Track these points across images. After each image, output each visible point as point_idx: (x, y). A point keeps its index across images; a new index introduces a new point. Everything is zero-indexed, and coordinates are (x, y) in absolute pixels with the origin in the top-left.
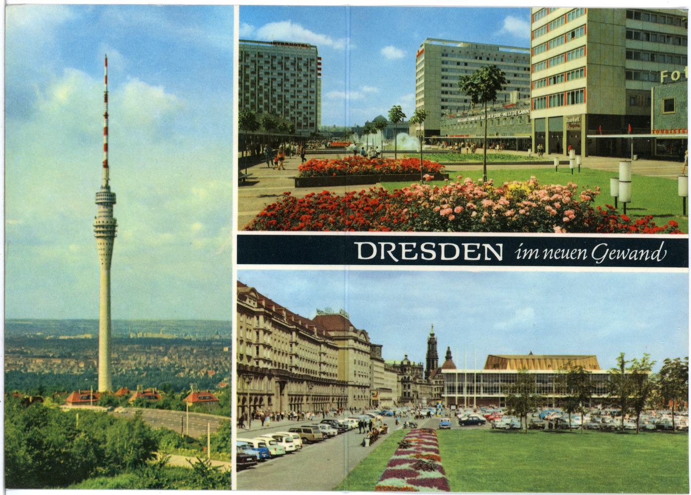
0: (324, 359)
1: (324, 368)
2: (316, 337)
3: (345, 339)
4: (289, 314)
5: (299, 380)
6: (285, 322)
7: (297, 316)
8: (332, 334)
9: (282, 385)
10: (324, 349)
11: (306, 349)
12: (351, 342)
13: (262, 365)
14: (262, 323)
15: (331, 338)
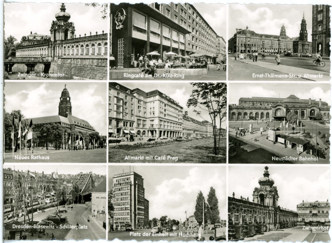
0: (203, 128)
1: (203, 129)
2: (202, 124)
3: (207, 125)
4: (196, 121)
5: (197, 131)
6: (196, 122)
7: (198, 121)
8: (205, 124)
9: (194, 132)
10: (203, 126)
11: (199, 126)
12: (208, 125)
13: (191, 129)
14: (191, 122)
15: (205, 125)
